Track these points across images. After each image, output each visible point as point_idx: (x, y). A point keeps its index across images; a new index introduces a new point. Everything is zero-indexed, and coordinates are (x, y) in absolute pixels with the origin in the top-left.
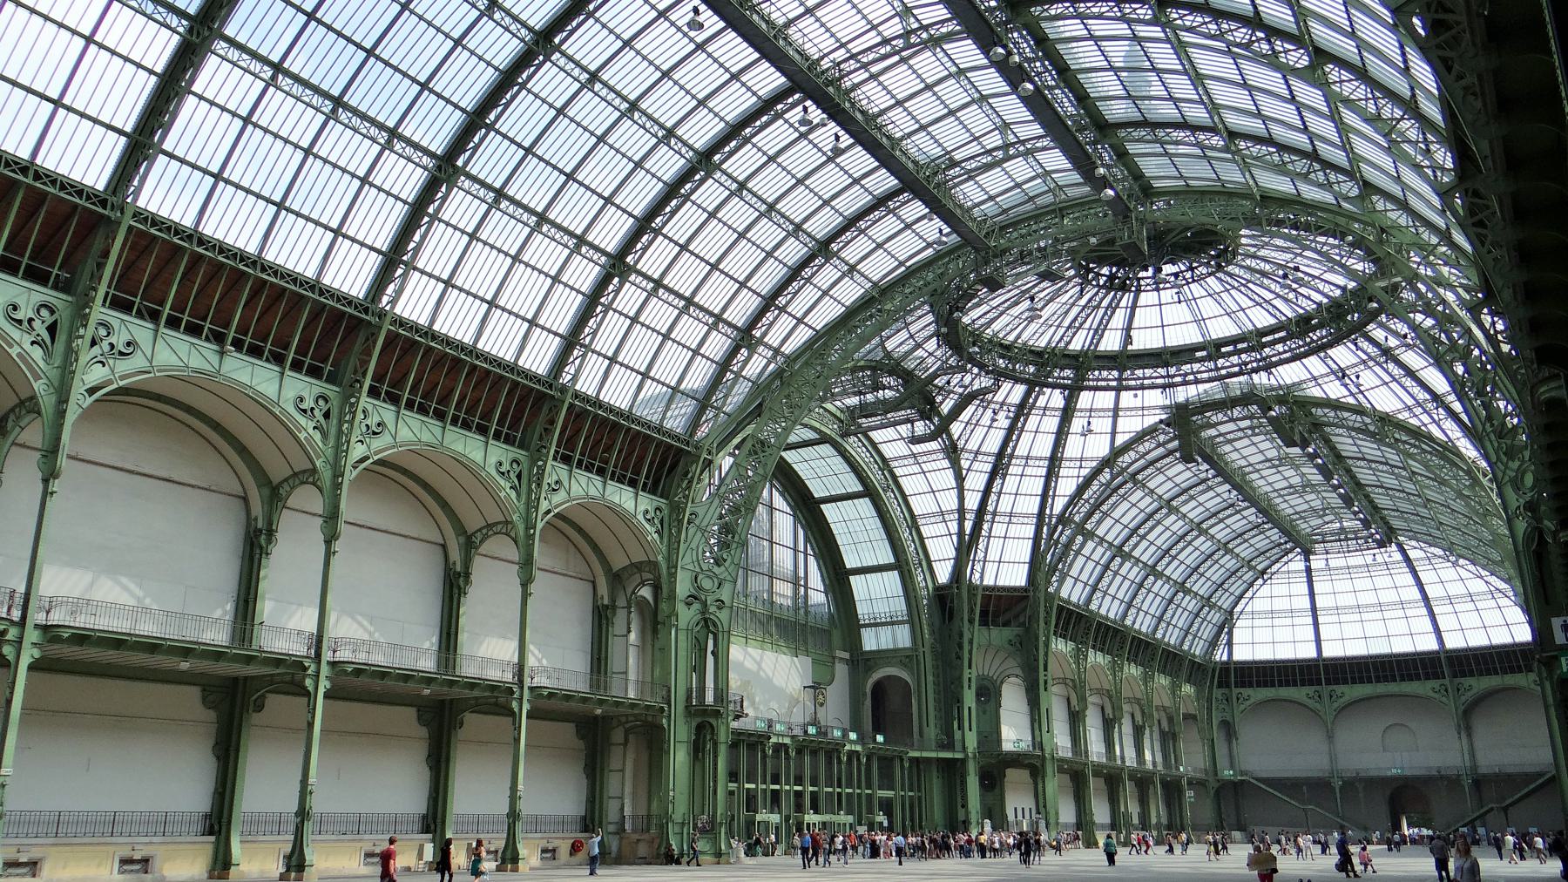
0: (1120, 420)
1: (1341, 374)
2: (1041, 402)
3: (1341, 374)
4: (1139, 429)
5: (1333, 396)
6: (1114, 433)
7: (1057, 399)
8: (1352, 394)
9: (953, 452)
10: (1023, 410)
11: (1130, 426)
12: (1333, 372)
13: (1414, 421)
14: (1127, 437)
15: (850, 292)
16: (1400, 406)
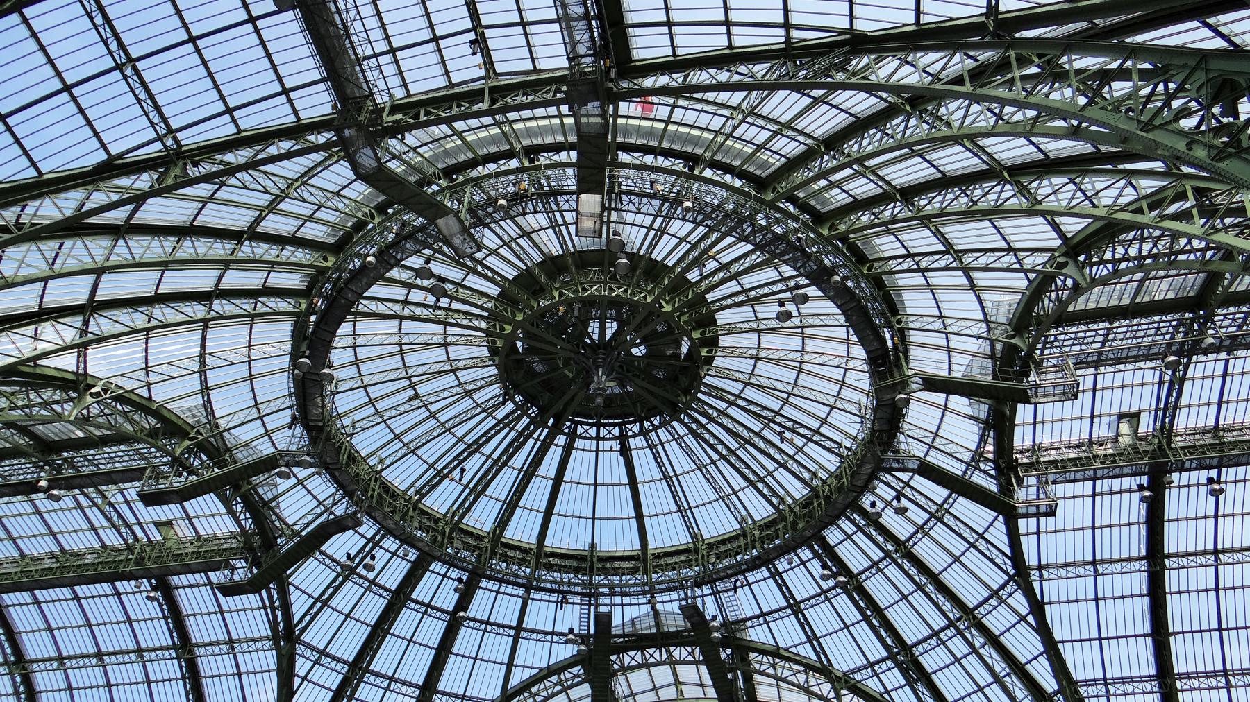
0: (522, 644)
1: (795, 607)
2: (422, 591)
3: (795, 607)
4: (544, 665)
5: (782, 645)
6: (510, 665)
7: (448, 599)
8: (810, 641)
9: (286, 638)
10: (399, 598)
11: (534, 655)
12: (789, 606)
13: (873, 685)
14: (527, 674)
15: (129, 133)
16: (861, 661)
